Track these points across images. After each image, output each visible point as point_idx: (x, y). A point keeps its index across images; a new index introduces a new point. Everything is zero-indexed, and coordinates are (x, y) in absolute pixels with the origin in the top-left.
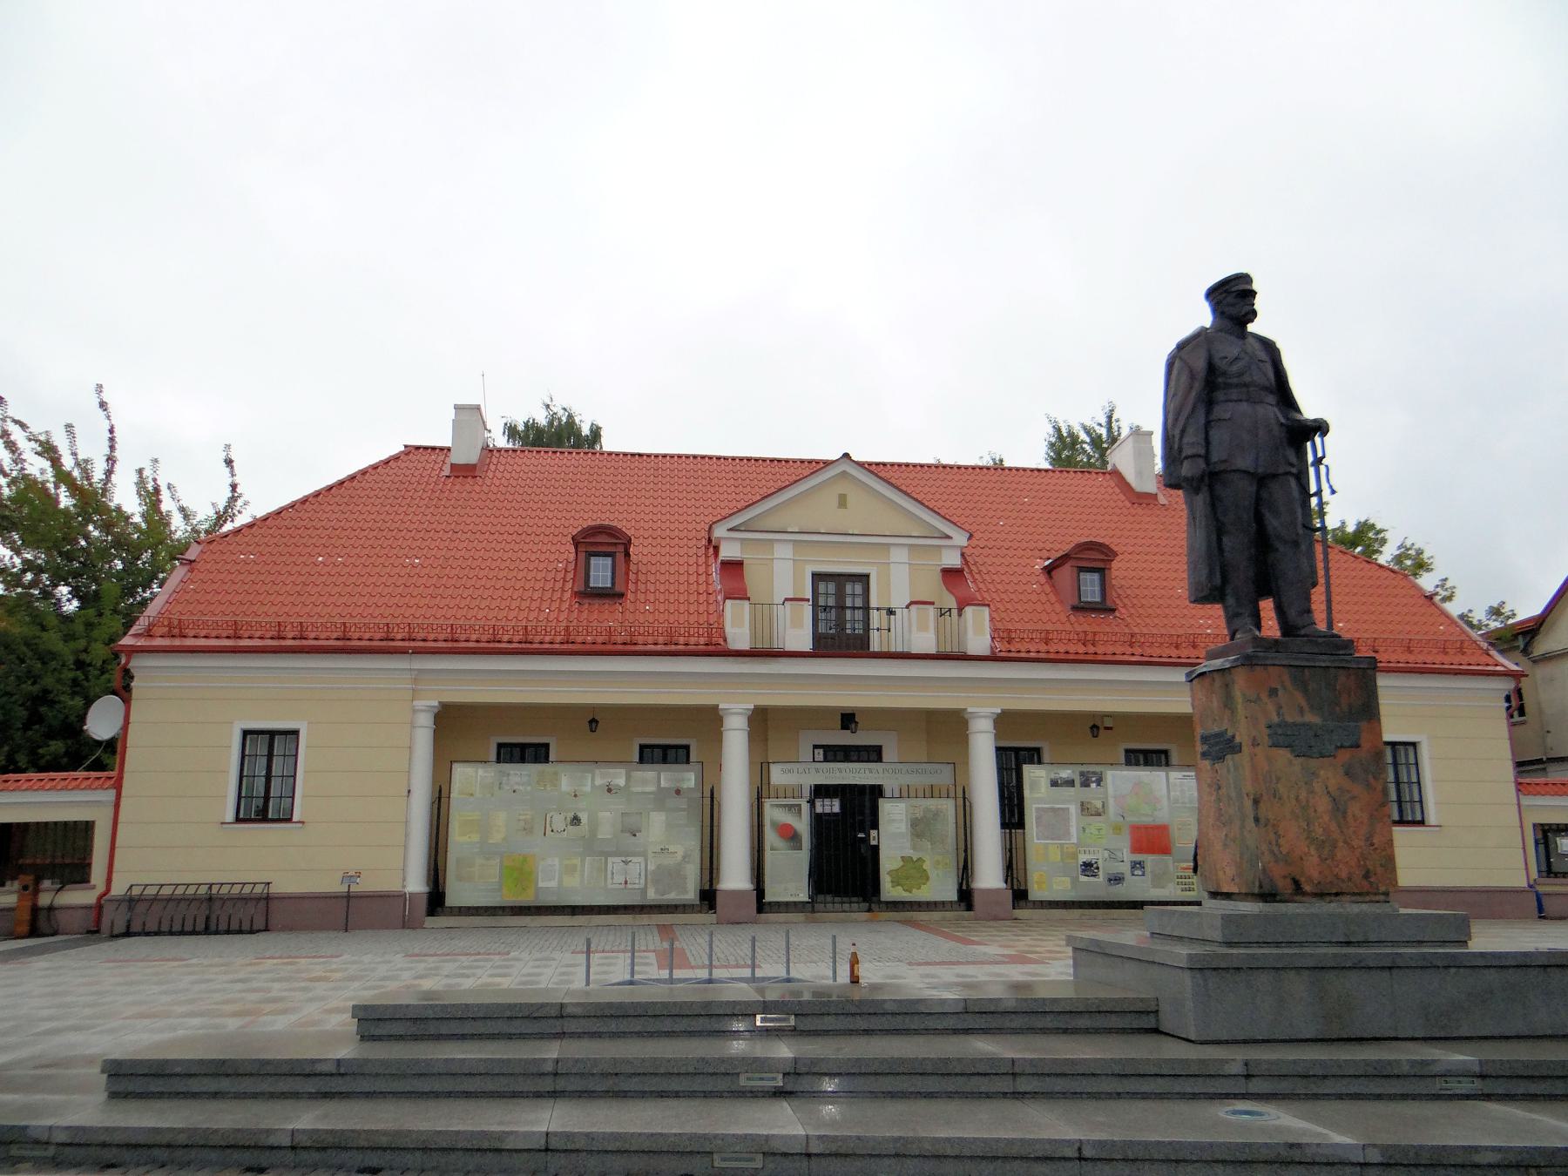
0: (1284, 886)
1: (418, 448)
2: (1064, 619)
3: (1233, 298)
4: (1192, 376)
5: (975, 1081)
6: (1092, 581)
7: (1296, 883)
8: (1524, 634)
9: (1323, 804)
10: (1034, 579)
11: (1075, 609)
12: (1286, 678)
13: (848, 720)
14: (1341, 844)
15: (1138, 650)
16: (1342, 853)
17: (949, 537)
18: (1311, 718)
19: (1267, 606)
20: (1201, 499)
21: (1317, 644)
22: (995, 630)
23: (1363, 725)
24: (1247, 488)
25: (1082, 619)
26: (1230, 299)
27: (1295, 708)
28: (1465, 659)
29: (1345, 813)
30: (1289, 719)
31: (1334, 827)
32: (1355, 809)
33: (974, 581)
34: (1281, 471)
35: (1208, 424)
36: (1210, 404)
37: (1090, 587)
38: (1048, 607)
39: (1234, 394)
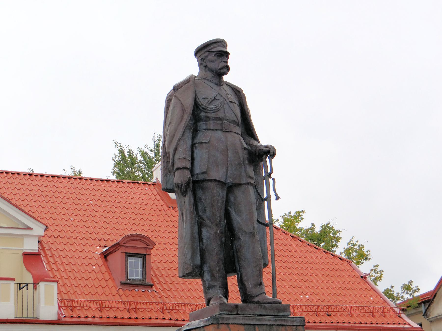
2: (114, 292)
3: (214, 56)
4: (183, 111)
6: (137, 263)
8: (424, 303)
10: (93, 262)
11: (123, 284)
17: (29, 228)
19: (233, 281)
20: (188, 200)
21: (265, 308)
22: (61, 301)
24: (220, 194)
25: (128, 293)
26: (211, 57)
28: (386, 320)
33: (48, 263)
34: (244, 181)
35: (193, 146)
36: (195, 131)
37: (135, 268)
38: (104, 283)
39: (212, 125)
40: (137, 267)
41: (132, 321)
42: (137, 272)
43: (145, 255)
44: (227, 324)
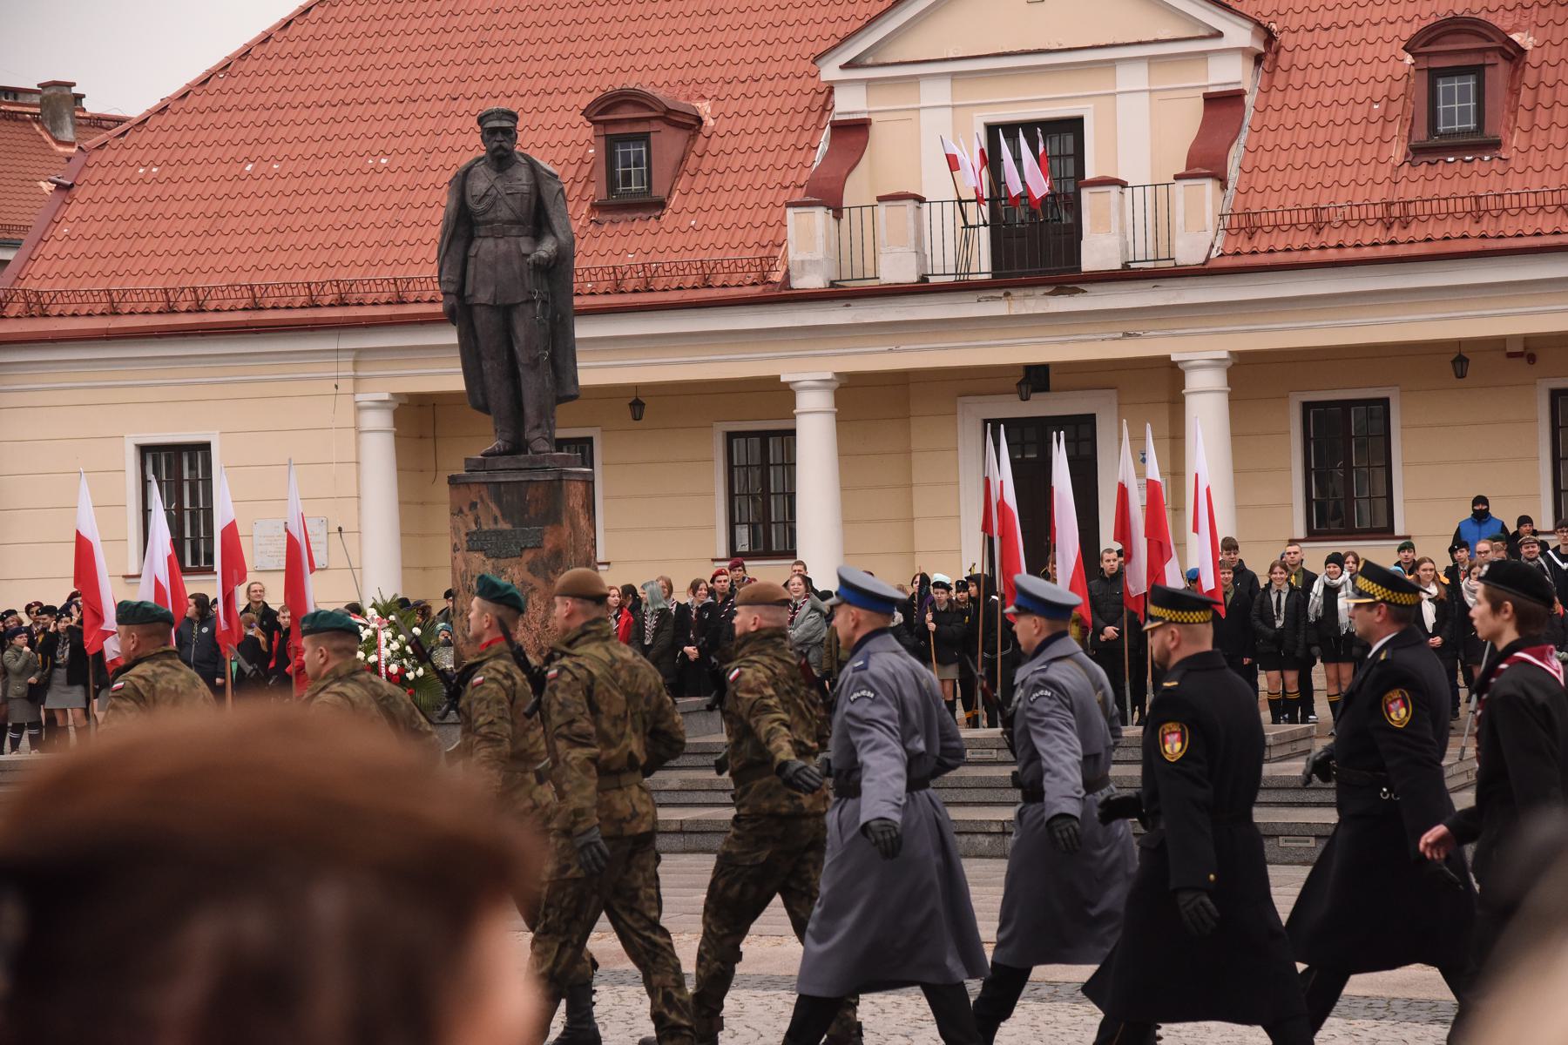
6: (1466, 89)
12: (484, 494)
13: (1036, 378)
15: (1487, 225)
17: (1219, 35)
23: (548, 528)
27: (492, 519)
30: (485, 528)
36: (470, 239)
40: (1464, 98)
41: (1385, 251)
42: (1464, 112)
43: (1483, 66)
44: (467, 484)
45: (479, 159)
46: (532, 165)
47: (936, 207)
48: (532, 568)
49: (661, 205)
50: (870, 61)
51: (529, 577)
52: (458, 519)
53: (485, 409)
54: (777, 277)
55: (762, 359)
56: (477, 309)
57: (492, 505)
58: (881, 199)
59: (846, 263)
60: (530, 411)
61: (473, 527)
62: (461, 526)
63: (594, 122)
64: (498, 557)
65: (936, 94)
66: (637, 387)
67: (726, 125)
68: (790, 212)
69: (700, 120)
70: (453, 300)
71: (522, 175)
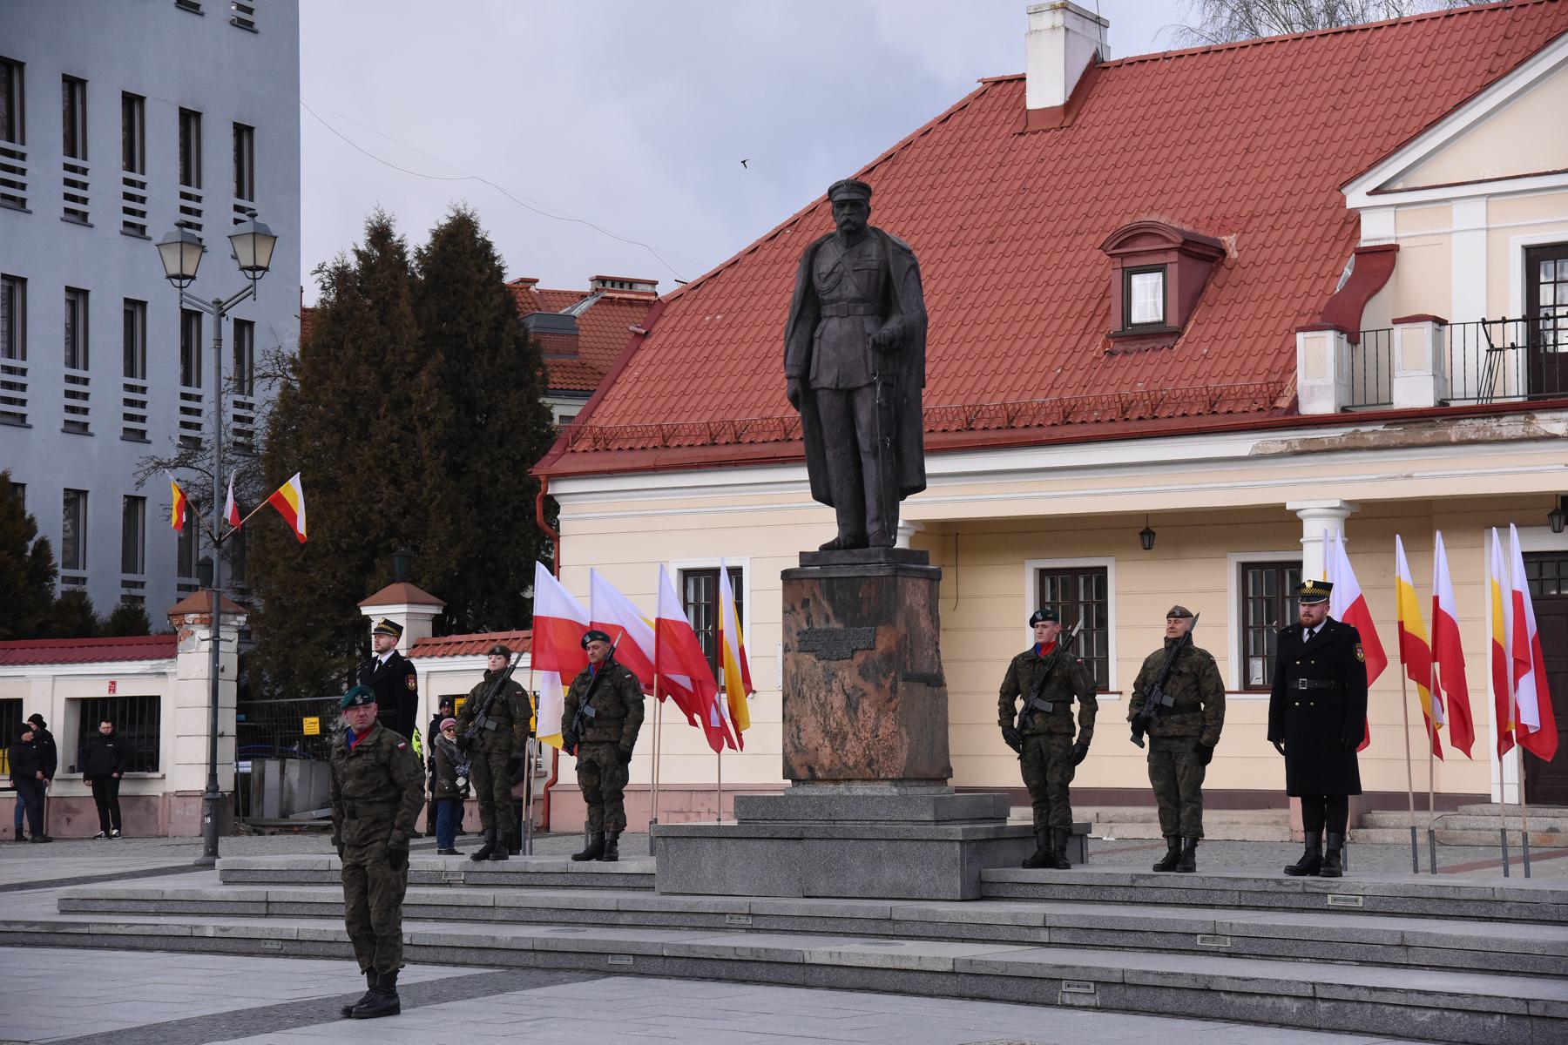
0: (803, 773)
1: (998, 82)
5: (475, 911)
7: (811, 769)
9: (838, 701)
14: (850, 736)
16: (851, 744)
18: (836, 625)
23: (881, 629)
29: (856, 710)
30: (817, 627)
31: (846, 721)
32: (865, 704)
45: (831, 236)
46: (884, 239)
47: (1458, 330)
48: (863, 672)
49: (1177, 333)
50: (1399, 186)
51: (860, 682)
52: (790, 617)
53: (829, 502)
54: (1283, 403)
55: (1264, 486)
56: (820, 393)
57: (825, 603)
58: (1396, 322)
59: (1359, 388)
60: (871, 502)
61: (805, 627)
62: (793, 624)
63: (1111, 256)
64: (829, 659)
65: (1469, 214)
66: (1147, 515)
67: (1251, 256)
68: (1300, 337)
69: (1223, 252)
70: (796, 385)
71: (873, 249)
